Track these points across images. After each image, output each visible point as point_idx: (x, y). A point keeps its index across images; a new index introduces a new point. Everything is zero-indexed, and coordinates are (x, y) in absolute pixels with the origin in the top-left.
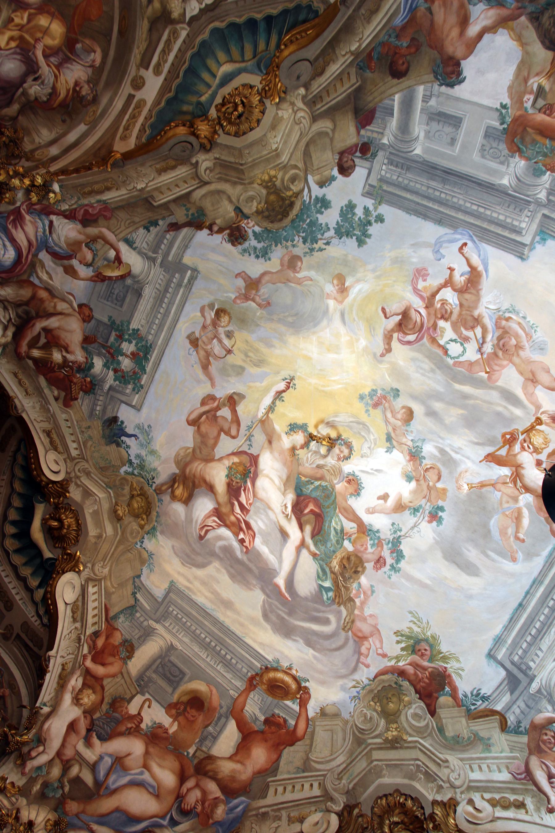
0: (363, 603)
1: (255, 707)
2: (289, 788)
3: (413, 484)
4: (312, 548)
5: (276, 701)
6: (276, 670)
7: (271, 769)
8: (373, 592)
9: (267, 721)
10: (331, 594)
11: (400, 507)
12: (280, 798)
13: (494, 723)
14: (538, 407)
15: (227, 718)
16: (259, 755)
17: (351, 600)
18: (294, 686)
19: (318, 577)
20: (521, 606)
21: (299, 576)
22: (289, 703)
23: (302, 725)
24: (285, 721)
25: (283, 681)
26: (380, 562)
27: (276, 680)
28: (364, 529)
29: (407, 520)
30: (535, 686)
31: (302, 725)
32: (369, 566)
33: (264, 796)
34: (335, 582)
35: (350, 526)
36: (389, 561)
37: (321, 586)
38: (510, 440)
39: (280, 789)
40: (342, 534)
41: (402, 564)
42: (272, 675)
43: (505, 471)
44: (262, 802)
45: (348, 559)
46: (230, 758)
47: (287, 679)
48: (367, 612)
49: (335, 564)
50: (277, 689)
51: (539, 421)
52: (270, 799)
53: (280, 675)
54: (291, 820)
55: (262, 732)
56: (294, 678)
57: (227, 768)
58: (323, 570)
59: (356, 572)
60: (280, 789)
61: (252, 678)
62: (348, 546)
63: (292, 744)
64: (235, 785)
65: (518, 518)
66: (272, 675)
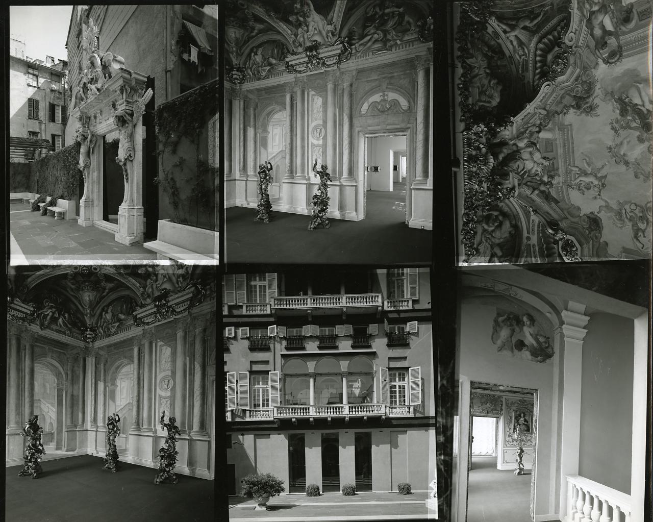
0: (613, 105)
1: (612, 41)
2: (585, 36)
3: (622, 154)
4: (639, 107)
5: (609, 51)
6: (618, 59)
7: (592, 35)
8: (613, 111)
9: (606, 43)
10: (624, 98)
11: (622, 143)
12: (583, 30)
13: (559, 110)
14: (602, 199)
15: (615, 29)
16: (598, 32)
17: (617, 102)
18: (610, 61)
19: (631, 100)
20: (573, 143)
21: (637, 94)
22: (606, 55)
23: (598, 53)
24: (603, 49)
25: (614, 58)
26: (617, 121)
27: (616, 56)
28: (628, 127)
29: (618, 141)
30: (557, 128)
31: (598, 53)
32: (619, 118)
33: (586, 26)
34: (625, 103)
35: (634, 125)
36: (614, 124)
37: (628, 97)
38: (604, 185)
39: (586, 33)
40: (634, 120)
41: (610, 127)
42: (618, 56)
43: (599, 175)
44: (585, 24)
45: (626, 114)
46: (602, 21)
47: (613, 61)
48: (610, 103)
49: (629, 108)
50: (612, 54)
51: (599, 195)
52: (584, 27)
53: (616, 59)
54: (576, 30)
55: (604, 39)
56: (612, 63)
57: (600, 17)
58: (630, 103)
59: (622, 112)
60: (586, 33)
61: (621, 49)
62: (629, 118)
63: (595, 46)
64: (593, 17)
65: (589, 165)
66: (618, 56)
